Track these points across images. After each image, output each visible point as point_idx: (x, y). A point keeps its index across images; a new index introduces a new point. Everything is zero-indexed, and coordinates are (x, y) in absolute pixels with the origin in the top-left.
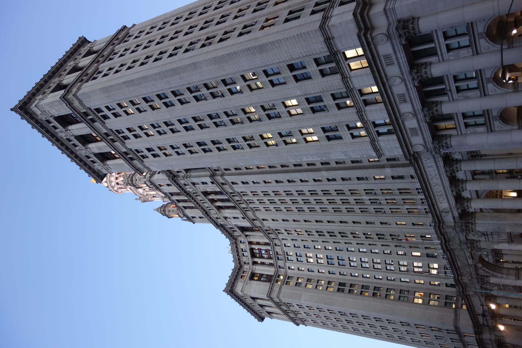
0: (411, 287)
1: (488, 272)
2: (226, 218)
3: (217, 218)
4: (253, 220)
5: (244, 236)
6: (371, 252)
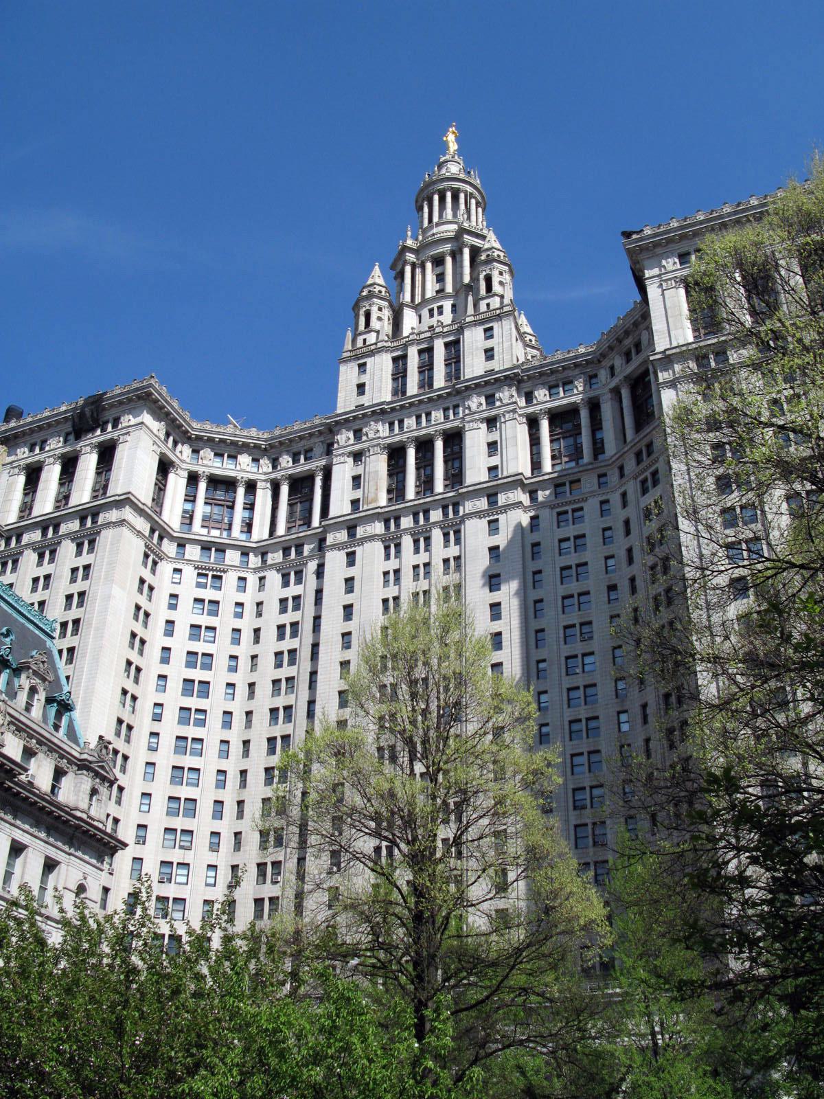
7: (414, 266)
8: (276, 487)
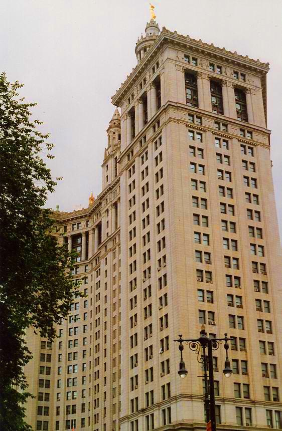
2: (107, 211)
4: (106, 247)
6: (83, 377)
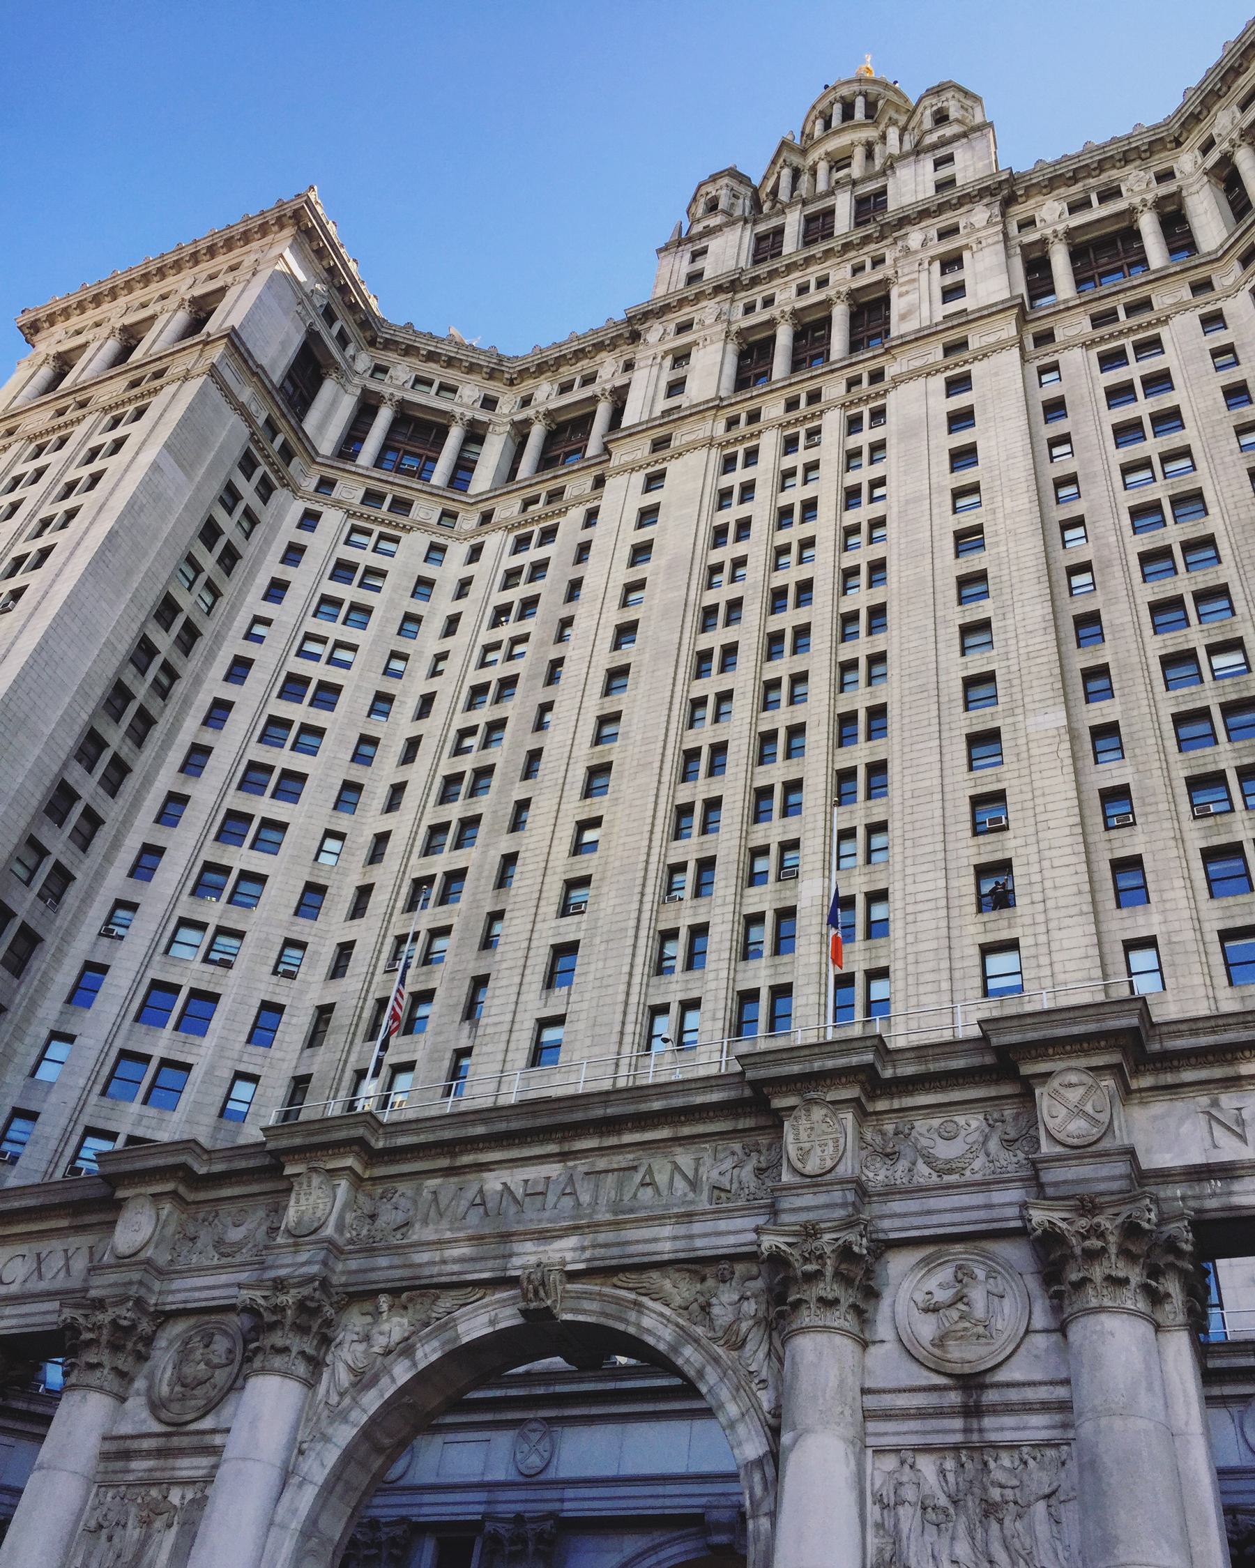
0: (33, 1004)
1: (363, 1380)
2: (681, 357)
3: (684, 328)
5: (529, 412)
7: (796, 174)
8: (520, 432)
